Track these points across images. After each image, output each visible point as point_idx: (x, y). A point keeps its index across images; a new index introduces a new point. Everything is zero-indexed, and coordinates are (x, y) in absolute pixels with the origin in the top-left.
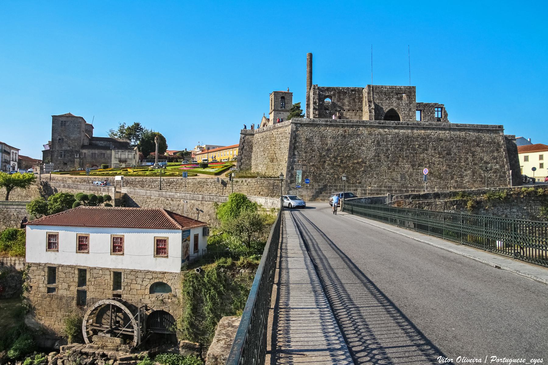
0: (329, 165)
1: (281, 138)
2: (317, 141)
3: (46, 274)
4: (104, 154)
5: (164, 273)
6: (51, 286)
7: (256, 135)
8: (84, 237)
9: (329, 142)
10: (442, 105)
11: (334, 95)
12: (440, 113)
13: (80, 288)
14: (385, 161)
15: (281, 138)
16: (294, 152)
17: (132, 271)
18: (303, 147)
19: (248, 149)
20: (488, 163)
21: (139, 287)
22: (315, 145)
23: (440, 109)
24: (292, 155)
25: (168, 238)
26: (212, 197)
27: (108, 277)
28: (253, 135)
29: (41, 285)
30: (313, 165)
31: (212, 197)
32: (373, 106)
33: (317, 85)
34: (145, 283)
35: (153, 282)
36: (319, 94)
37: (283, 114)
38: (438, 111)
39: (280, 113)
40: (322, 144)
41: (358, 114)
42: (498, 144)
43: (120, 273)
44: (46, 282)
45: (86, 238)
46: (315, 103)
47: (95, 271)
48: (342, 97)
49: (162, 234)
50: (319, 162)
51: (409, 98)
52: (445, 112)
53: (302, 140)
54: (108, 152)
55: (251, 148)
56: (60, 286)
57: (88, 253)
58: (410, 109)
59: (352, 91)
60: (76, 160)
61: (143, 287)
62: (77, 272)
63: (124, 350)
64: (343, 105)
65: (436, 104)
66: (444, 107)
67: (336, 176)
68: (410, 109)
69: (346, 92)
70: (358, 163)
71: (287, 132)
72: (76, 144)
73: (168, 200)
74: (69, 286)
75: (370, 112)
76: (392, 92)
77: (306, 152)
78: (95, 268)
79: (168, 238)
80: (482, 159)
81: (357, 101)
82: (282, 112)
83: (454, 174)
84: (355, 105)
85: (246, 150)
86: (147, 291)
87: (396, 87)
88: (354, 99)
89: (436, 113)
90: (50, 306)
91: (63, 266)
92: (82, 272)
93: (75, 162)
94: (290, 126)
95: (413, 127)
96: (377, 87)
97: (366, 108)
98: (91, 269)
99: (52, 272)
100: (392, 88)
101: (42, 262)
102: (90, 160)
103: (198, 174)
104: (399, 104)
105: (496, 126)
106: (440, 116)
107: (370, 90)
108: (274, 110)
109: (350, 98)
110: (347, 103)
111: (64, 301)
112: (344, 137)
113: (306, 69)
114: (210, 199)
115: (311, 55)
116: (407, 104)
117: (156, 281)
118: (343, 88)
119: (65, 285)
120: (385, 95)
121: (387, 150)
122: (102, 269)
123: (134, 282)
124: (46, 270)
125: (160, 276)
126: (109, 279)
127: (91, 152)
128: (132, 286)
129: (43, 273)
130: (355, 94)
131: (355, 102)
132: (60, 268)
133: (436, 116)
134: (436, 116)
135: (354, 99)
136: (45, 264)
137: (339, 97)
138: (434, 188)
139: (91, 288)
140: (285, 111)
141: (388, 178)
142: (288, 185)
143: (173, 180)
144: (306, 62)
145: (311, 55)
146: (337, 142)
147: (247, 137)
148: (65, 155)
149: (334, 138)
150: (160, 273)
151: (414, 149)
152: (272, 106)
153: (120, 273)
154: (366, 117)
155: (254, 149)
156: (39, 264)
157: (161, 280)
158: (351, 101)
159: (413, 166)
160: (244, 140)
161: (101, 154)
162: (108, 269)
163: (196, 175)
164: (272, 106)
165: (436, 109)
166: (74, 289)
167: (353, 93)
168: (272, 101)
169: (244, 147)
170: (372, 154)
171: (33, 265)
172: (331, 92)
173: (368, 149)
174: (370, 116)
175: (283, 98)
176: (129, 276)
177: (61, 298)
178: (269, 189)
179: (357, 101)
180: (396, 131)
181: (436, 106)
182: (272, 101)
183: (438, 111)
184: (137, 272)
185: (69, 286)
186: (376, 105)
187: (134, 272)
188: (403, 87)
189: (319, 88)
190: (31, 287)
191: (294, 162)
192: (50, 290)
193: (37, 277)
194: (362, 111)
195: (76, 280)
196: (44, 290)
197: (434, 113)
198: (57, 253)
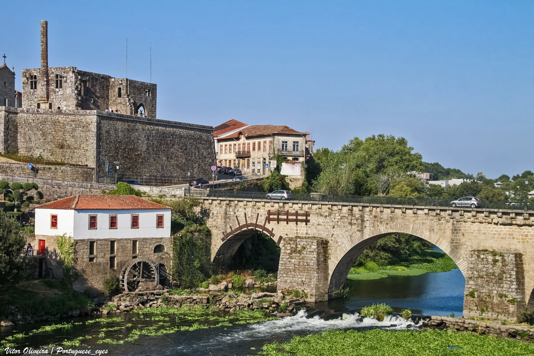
0: (121, 156)
1: (73, 125)
5: (162, 238)
6: (92, 256)
7: (18, 115)
9: (120, 135)
11: (89, 80)
14: (153, 154)
15: (73, 125)
16: (99, 143)
17: (144, 239)
18: (105, 138)
19: (13, 129)
20: (205, 157)
22: (112, 137)
24: (98, 147)
25: (164, 215)
26: (100, 186)
28: (17, 113)
29: (85, 257)
30: (112, 156)
31: (100, 186)
33: (76, 68)
34: (151, 246)
40: (116, 137)
44: (88, 254)
45: (115, 217)
47: (121, 241)
48: (94, 83)
49: (160, 213)
50: (115, 153)
53: (104, 132)
55: (16, 127)
57: (117, 228)
59: (102, 78)
63: (159, 288)
64: (96, 90)
67: (126, 166)
68: (153, 105)
69: (97, 79)
70: (138, 155)
73: (54, 187)
74: (105, 255)
77: (107, 144)
78: (121, 239)
79: (164, 215)
83: (189, 167)
85: (11, 130)
88: (103, 87)
90: (92, 272)
91: (100, 240)
95: (166, 125)
100: (142, 83)
101: (85, 238)
105: (208, 127)
107: (127, 84)
109: (100, 85)
110: (98, 90)
111: (102, 266)
112: (129, 130)
113: (39, 38)
114: (99, 187)
115: (46, 23)
117: (158, 244)
118: (96, 74)
120: (138, 90)
121: (153, 144)
122: (126, 239)
126: (130, 245)
129: (86, 247)
130: (104, 81)
131: (104, 90)
132: (98, 241)
136: (88, 239)
137: (92, 83)
141: (155, 169)
142: (98, 173)
144: (40, 29)
146: (125, 135)
147: (10, 115)
149: (122, 131)
151: (168, 145)
155: (19, 130)
157: (160, 243)
159: (168, 158)
160: (8, 119)
162: (129, 239)
166: (108, 256)
169: (9, 126)
170: (144, 148)
171: (79, 241)
174: (131, 109)
177: (100, 264)
178: (83, 176)
179: (105, 89)
180: (157, 127)
184: (146, 239)
185: (105, 255)
188: (149, 84)
190: (77, 259)
191: (100, 151)
192: (91, 259)
193: (82, 251)
196: (86, 260)
198: (96, 230)
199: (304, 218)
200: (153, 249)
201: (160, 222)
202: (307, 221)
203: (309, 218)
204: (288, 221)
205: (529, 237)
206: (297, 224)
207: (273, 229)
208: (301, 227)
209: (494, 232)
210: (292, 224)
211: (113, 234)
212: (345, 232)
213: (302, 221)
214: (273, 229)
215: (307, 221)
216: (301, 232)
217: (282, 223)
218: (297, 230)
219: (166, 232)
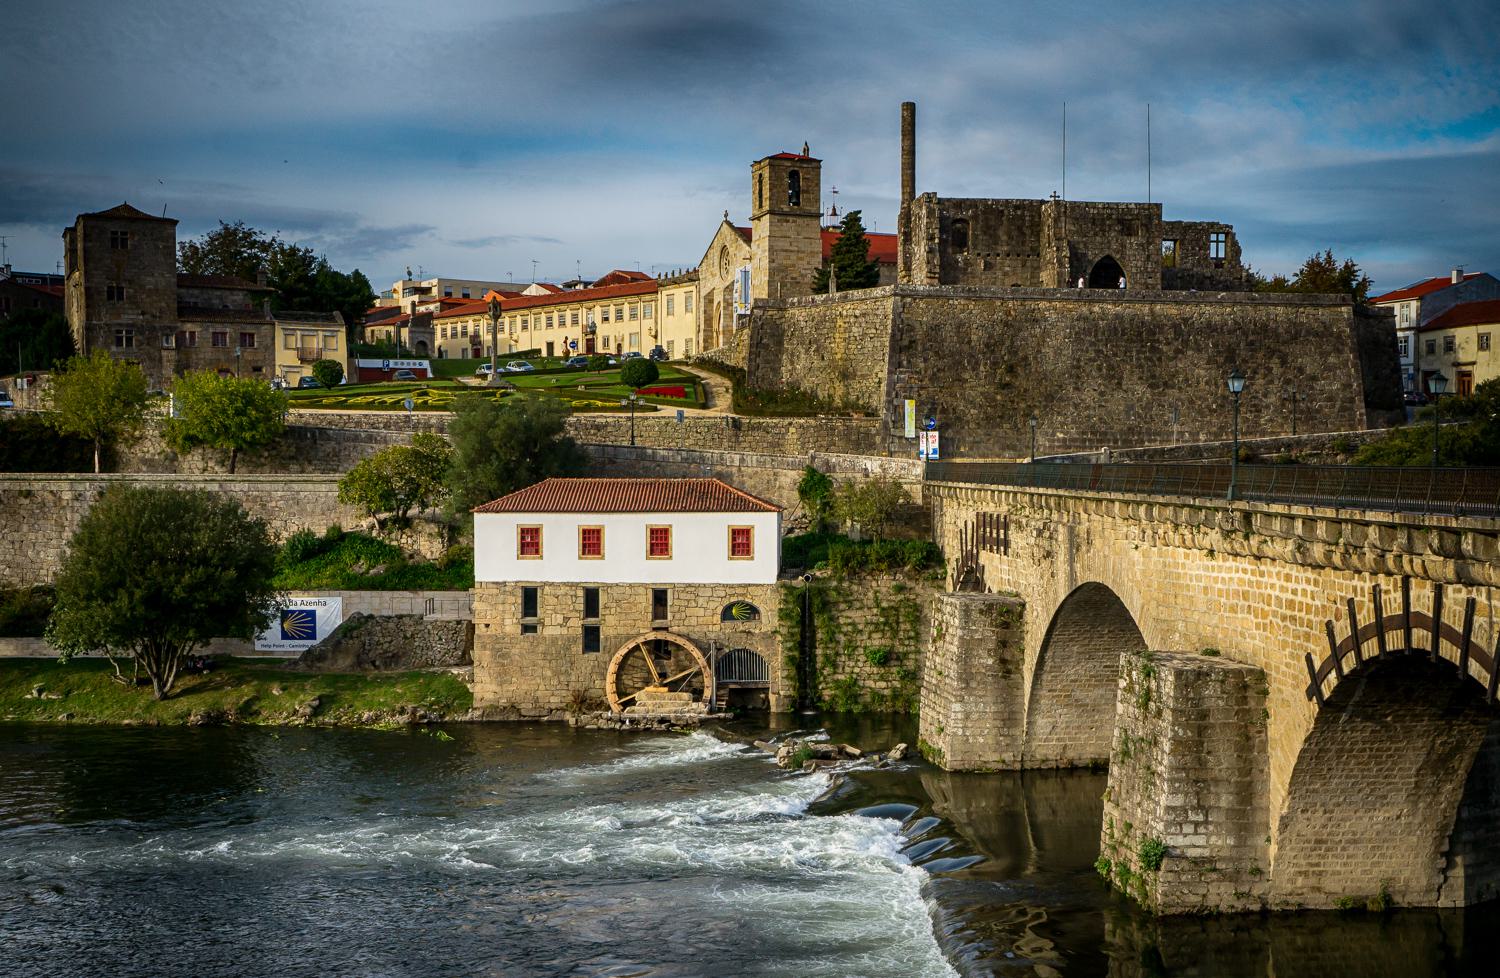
2: (948, 332)
3: (520, 601)
4: (252, 336)
6: (530, 620)
8: (594, 531)
10: (1227, 226)
11: (975, 217)
12: (1222, 246)
13: (591, 621)
17: (690, 585)
20: (1314, 378)
21: (701, 612)
23: (1222, 237)
27: (642, 599)
32: (1066, 253)
34: (712, 605)
35: (726, 602)
36: (942, 219)
37: (794, 222)
38: (1217, 242)
39: (788, 221)
41: (1028, 264)
42: (1339, 336)
43: (664, 592)
46: (931, 238)
51: (1147, 231)
52: (1235, 244)
54: (265, 329)
56: (547, 621)
58: (1148, 256)
59: (1017, 207)
60: (164, 353)
61: (709, 612)
62: (581, 593)
65: (1212, 225)
66: (1234, 231)
68: (1148, 256)
69: (1002, 211)
71: (878, 312)
72: (163, 304)
75: (1061, 264)
76: (1110, 216)
80: (1301, 370)
81: (1028, 232)
82: (791, 219)
84: (1023, 243)
86: (717, 618)
87: (1117, 204)
88: (1020, 229)
89: (1213, 246)
91: (552, 584)
92: (591, 596)
93: (165, 359)
94: (889, 304)
96: (1075, 205)
97: (1050, 254)
98: (610, 586)
99: (530, 597)
100: (1107, 206)
102: (209, 356)
103: (659, 407)
104: (1123, 246)
106: (1222, 255)
108: (771, 212)
110: (1004, 238)
116: (1142, 245)
118: (997, 201)
119: (560, 619)
122: (631, 586)
123: (694, 604)
124: (519, 593)
125: (739, 591)
126: (646, 601)
127: (211, 330)
128: (689, 612)
129: (512, 599)
133: (1213, 254)
134: (1213, 254)
135: (1020, 229)
138: (1198, 434)
139: (611, 620)
140: (800, 215)
143: (604, 420)
145: (910, 109)
148: (129, 341)
150: (740, 586)
152: (761, 196)
153: (664, 592)
154: (1047, 277)
156: (504, 584)
158: (1015, 233)
161: (243, 335)
163: (656, 409)
164: (761, 196)
165: (1213, 237)
166: (577, 624)
167: (1019, 212)
168: (760, 182)
172: (968, 210)
173: (1058, 352)
175: (794, 175)
176: (682, 596)
181: (1213, 227)
182: (760, 182)
183: (1217, 242)
185: (566, 619)
186: (1072, 247)
187: (692, 589)
188: (1133, 206)
189: (940, 201)
194: (1038, 255)
195: (581, 607)
197: (1209, 248)
200: (720, 610)
201: (741, 542)
211: (591, 572)
219: (763, 567)
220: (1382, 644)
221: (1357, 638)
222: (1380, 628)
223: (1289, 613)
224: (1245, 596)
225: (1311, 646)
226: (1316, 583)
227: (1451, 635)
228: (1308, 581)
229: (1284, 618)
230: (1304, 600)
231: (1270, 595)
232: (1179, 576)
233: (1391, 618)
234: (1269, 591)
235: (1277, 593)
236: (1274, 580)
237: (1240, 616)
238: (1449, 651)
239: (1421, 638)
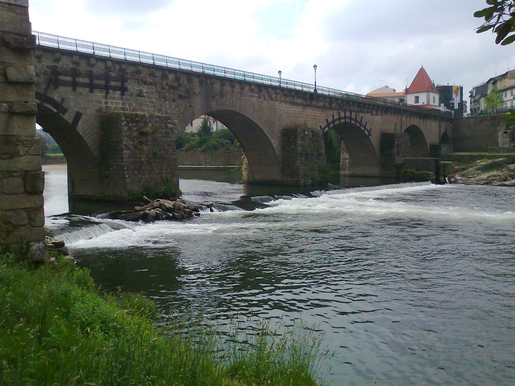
199: (119, 84)
202: (123, 90)
203: (127, 85)
204: (92, 87)
205: (309, 116)
206: (107, 93)
207: (63, 100)
208: (114, 98)
209: (292, 111)
210: (99, 95)
212: (175, 108)
213: (115, 89)
214: (63, 100)
215: (123, 90)
216: (113, 106)
217: (79, 89)
218: (107, 103)
220: (345, 120)
221: (334, 121)
222: (340, 119)
223: (314, 118)
224: (300, 114)
225: (320, 124)
226: (322, 111)
227: (353, 120)
228: (320, 111)
229: (312, 119)
230: (319, 115)
231: (308, 114)
232: (276, 109)
233: (342, 117)
234: (307, 113)
235: (310, 113)
236: (309, 111)
237: (298, 119)
238: (353, 122)
239: (348, 120)
